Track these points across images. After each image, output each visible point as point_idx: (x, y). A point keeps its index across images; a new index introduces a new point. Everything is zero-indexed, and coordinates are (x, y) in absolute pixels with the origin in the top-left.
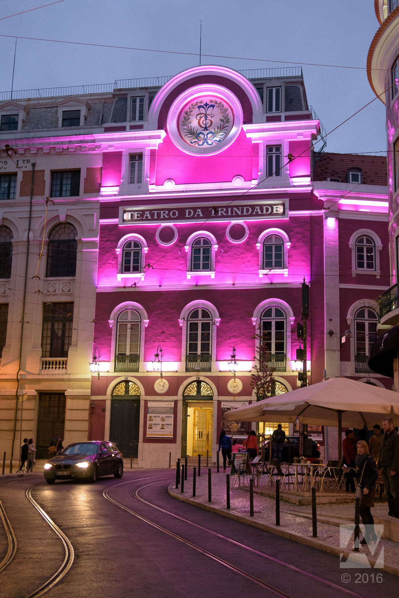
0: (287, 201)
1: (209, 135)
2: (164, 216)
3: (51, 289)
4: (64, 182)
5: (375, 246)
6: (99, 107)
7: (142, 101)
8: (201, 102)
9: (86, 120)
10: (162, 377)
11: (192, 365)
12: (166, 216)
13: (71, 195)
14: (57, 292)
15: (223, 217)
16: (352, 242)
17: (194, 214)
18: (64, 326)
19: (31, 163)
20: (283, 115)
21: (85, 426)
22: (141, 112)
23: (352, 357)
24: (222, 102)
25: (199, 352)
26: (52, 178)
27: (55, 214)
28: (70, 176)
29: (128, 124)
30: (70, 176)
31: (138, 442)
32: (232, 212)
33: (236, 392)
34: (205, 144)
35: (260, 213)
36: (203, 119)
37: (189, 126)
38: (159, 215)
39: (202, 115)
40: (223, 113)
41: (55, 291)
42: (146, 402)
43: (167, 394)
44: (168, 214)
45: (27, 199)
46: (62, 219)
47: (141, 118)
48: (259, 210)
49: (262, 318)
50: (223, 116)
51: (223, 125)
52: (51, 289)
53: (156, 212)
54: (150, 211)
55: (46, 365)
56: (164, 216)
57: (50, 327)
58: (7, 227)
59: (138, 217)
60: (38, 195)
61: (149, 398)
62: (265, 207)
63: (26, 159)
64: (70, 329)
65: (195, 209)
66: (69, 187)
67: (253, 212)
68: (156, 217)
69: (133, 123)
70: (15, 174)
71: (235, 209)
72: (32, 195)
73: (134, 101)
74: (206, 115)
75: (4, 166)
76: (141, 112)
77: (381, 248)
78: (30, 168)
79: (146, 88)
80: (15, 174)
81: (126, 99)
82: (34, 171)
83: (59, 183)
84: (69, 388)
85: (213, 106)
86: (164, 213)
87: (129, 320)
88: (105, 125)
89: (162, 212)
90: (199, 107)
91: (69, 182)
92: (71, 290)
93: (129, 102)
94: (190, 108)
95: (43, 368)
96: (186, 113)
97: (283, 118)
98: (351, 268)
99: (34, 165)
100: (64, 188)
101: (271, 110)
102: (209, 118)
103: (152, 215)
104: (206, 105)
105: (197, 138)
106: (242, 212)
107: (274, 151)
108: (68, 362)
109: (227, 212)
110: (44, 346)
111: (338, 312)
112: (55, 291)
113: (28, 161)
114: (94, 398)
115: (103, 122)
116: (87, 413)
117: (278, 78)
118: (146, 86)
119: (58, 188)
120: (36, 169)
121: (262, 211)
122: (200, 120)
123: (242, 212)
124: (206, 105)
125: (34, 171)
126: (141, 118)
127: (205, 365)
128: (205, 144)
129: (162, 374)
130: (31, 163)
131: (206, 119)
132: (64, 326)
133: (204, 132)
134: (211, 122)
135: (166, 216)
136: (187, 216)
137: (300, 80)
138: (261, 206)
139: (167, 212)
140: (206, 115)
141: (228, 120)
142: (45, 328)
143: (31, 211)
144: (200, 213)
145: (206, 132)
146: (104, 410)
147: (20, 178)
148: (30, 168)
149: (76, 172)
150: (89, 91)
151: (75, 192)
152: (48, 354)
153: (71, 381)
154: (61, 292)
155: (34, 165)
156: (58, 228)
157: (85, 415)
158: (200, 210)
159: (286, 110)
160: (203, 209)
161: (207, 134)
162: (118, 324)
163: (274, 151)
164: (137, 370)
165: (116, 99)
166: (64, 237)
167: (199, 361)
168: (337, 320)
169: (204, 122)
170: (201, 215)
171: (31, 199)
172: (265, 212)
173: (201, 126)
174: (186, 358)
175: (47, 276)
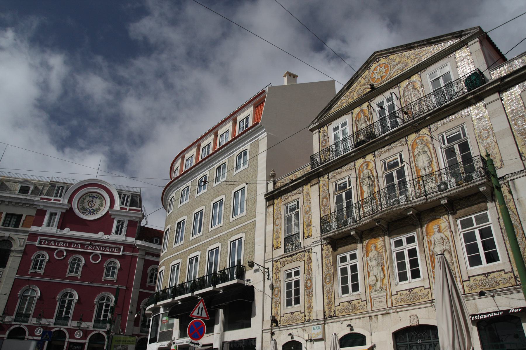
4: (13, 220)
6: (41, 188)
16: (149, 271)
22: (61, 194)
23: (140, 325)
26: (6, 217)
27: (2, 235)
28: (16, 217)
30: (16, 217)
47: (60, 197)
65: (77, 244)
66: (14, 223)
69: (56, 198)
76: (61, 194)
79: (67, 183)
81: (55, 187)
83: (9, 219)
85: (97, 198)
91: (15, 220)
93: (56, 188)
97: (128, 210)
98: (146, 282)
100: (11, 223)
101: (123, 204)
103: (55, 243)
106: (100, 249)
111: (137, 302)
119: (8, 222)
123: (100, 249)
126: (60, 197)
138: (110, 248)
145: (91, 209)
149: (20, 216)
150: (37, 179)
151: (17, 225)
159: (130, 206)
164: (27, 322)
168: (135, 306)
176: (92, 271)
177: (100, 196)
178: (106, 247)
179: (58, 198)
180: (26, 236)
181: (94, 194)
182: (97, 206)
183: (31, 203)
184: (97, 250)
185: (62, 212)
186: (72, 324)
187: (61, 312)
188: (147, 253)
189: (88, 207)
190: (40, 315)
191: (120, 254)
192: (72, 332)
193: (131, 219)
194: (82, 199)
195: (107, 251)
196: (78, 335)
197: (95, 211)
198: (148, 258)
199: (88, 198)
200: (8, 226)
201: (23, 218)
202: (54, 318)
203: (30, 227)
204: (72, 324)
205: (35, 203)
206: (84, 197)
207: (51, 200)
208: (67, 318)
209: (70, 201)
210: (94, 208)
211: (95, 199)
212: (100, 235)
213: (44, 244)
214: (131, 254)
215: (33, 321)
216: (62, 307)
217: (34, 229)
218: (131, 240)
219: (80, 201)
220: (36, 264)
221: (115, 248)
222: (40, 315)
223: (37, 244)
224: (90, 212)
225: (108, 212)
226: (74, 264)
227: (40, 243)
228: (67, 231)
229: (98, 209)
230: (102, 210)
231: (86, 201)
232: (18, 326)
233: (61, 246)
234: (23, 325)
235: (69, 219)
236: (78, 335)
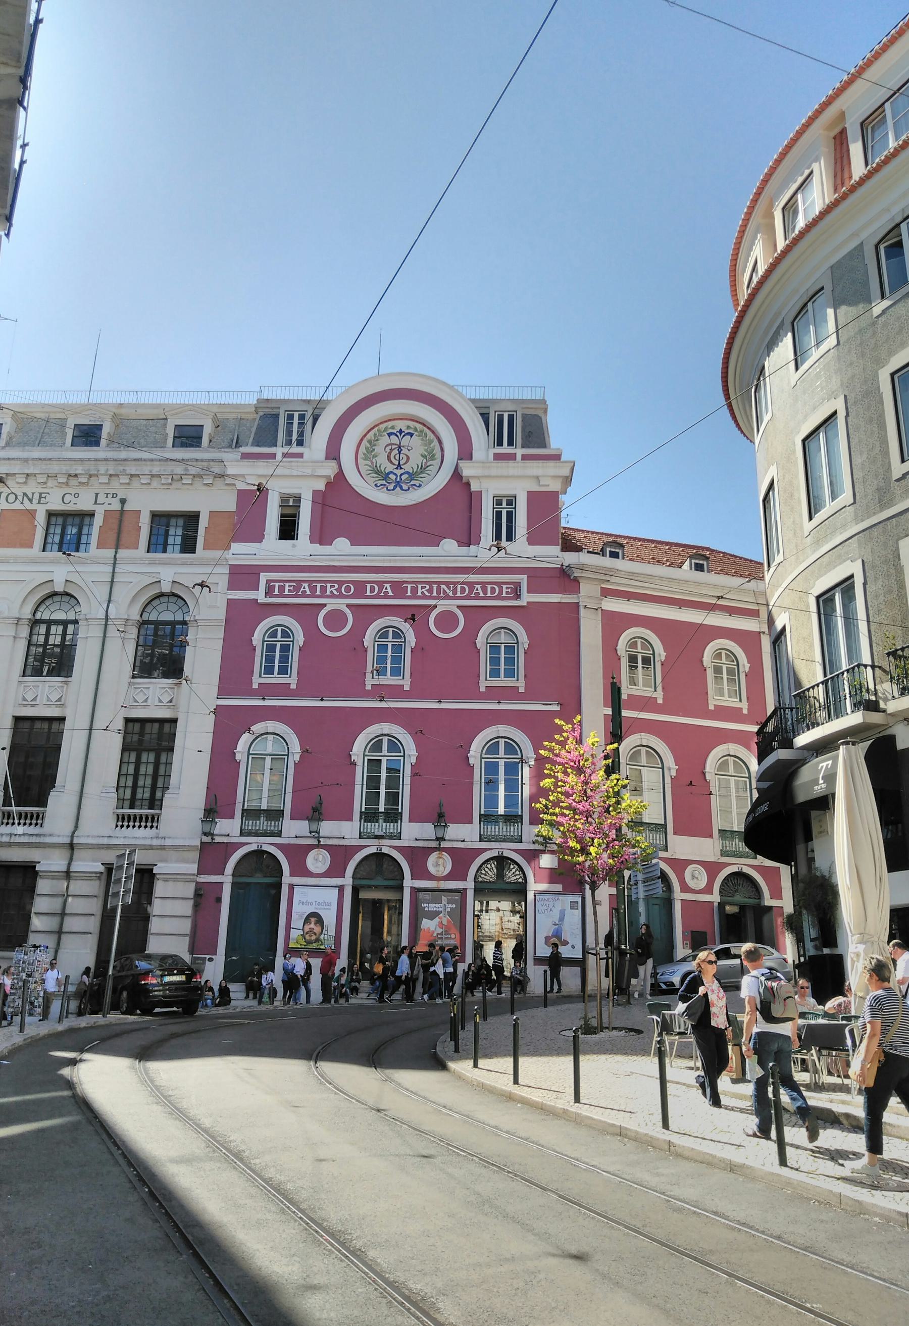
0: (523, 579)
1: (404, 477)
2: (331, 592)
3: (140, 698)
5: (654, 654)
7: (302, 417)
8: (393, 427)
9: (210, 441)
10: (319, 846)
11: (369, 827)
12: (335, 592)
13: (181, 552)
14: (149, 702)
15: (424, 597)
17: (380, 592)
18: (157, 758)
19: (118, 497)
20: (520, 452)
21: (186, 926)
22: (301, 434)
24: (425, 428)
25: (382, 808)
29: (279, 451)
30: (181, 522)
31: (275, 956)
32: (438, 592)
33: (439, 874)
34: (398, 488)
35: (482, 595)
36: (396, 451)
37: (374, 460)
38: (324, 589)
39: (394, 447)
40: (425, 445)
41: (146, 701)
42: (292, 887)
43: (327, 874)
44: (339, 590)
45: (110, 553)
46: (166, 588)
47: (300, 443)
48: (480, 591)
49: (484, 756)
50: (426, 450)
51: (426, 463)
52: (140, 698)
53: (319, 585)
54: (310, 582)
55: (123, 820)
56: (331, 592)
57: (133, 758)
58: (72, 596)
59: (289, 591)
60: (127, 548)
61: (296, 880)
62: (489, 587)
63: (111, 491)
64: (169, 764)
65: (381, 584)
66: (178, 540)
67: (471, 591)
68: (318, 593)
70: (92, 515)
71: (443, 586)
72: (117, 547)
73: (290, 417)
74: (400, 447)
75: (74, 500)
76: (301, 434)
77: (663, 659)
78: (116, 506)
80: (92, 515)
81: (277, 416)
82: (122, 512)
84: (161, 861)
85: (411, 435)
86: (332, 587)
87: (269, 751)
88: (243, 449)
89: (329, 585)
90: (390, 435)
91: (180, 531)
92: (174, 701)
94: (375, 435)
95: (117, 826)
96: (370, 442)
97: (519, 457)
99: (123, 501)
100: (171, 540)
101: (500, 443)
102: (404, 451)
103: (313, 589)
104: (401, 431)
105: (385, 479)
107: (504, 505)
108: (162, 818)
109: (431, 591)
110: (121, 790)
112: (146, 701)
113: (114, 495)
114: (203, 879)
115: (238, 445)
116: (191, 903)
117: (514, 401)
118: (308, 398)
120: (127, 507)
121: (485, 592)
122: (390, 453)
124: (401, 431)
125: (122, 512)
126: (300, 443)
127: (391, 827)
128: (398, 488)
129: (319, 842)
130: (118, 497)
131: (400, 453)
132: (157, 758)
133: (395, 471)
134: (408, 458)
135: (335, 592)
136: (368, 593)
137: (543, 406)
138: (484, 585)
139: (337, 586)
140: (400, 447)
141: (434, 455)
142: (125, 759)
143: (114, 572)
144: (389, 590)
145: (399, 472)
146: (219, 900)
147: (98, 521)
148: (116, 506)
149: (192, 519)
150: (216, 399)
151: (189, 546)
152: (127, 804)
153: (164, 849)
154: (157, 703)
155: (123, 501)
156: (156, 602)
157: (187, 908)
158: (388, 586)
160: (396, 585)
161: (401, 475)
162: (250, 757)
163: (504, 505)
164: (279, 834)
165: (262, 414)
166: (167, 617)
167: (380, 821)
169: (397, 457)
170: (391, 594)
171: (116, 553)
172: (489, 594)
173: (391, 462)
174: (361, 816)
175: (133, 677)
176: (445, 663)
177: (419, 426)
178: (471, 585)
179: (295, 449)
180: (220, 578)
181: (400, 425)
182: (415, 462)
183: (217, 469)
184: (447, 597)
185: (315, 493)
186: (414, 832)
187: (373, 797)
188: (606, 593)
189: (390, 468)
190: (315, 810)
191: (523, 602)
192: (418, 856)
193: (535, 488)
194: (365, 443)
195: (477, 597)
196: (439, 864)
197: (412, 476)
198: (613, 605)
199: (385, 440)
200: (165, 551)
201: (203, 523)
202: (356, 816)
203: (228, 548)
204: (414, 832)
205: (230, 471)
206: (371, 436)
207: (273, 456)
208: (393, 816)
209: (333, 453)
210: (407, 468)
211: (406, 441)
212: (449, 550)
213: (281, 595)
214: (555, 598)
215: (294, 830)
216: (373, 782)
217: (243, 552)
218: (550, 555)
219: (362, 449)
220: (270, 659)
221: (500, 584)
222: (315, 810)
223: (260, 596)
224: (398, 484)
225: (457, 475)
226: (382, 648)
227: (269, 592)
228: (342, 549)
229: (423, 469)
230: (434, 469)
231: (380, 448)
232: (254, 847)
233: (332, 596)
234: (267, 844)
235: (339, 510)
236: (439, 864)
